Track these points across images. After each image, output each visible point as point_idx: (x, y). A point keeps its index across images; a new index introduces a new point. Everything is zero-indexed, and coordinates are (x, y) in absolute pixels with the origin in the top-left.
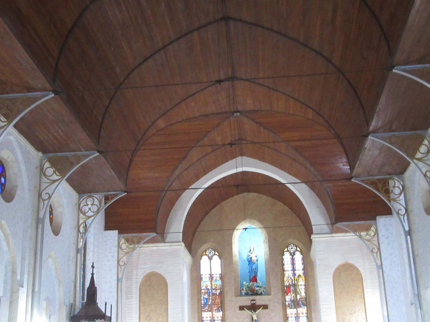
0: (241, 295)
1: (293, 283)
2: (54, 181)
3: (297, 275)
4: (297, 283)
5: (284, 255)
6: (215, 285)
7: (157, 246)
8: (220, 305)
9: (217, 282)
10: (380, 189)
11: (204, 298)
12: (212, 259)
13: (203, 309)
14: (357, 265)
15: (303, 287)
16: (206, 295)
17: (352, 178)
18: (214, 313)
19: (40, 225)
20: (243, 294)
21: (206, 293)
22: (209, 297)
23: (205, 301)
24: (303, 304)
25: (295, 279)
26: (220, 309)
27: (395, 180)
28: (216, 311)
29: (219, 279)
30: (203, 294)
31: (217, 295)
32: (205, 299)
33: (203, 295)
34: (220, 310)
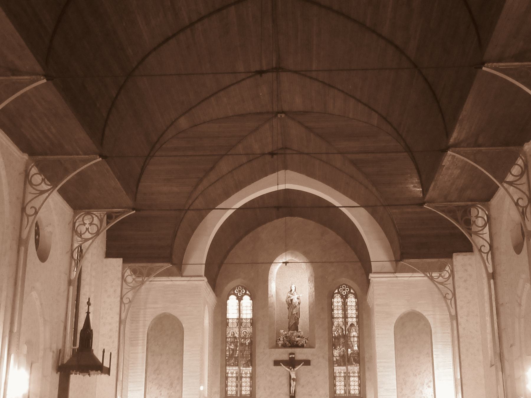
0: (277, 346)
1: (343, 333)
3: (349, 324)
4: (348, 334)
5: (334, 299)
6: (245, 332)
7: (172, 281)
8: (250, 358)
9: (247, 329)
11: (229, 348)
12: (242, 299)
13: (228, 363)
14: (425, 314)
15: (356, 339)
16: (232, 345)
17: (424, 203)
18: (241, 368)
19: (23, 249)
20: (280, 345)
21: (233, 342)
22: (236, 348)
23: (231, 352)
24: (355, 360)
25: (347, 328)
26: (249, 363)
27: (478, 208)
28: (245, 366)
29: (249, 325)
30: (228, 344)
31: (246, 346)
32: (231, 350)
33: (229, 345)
34: (250, 365)
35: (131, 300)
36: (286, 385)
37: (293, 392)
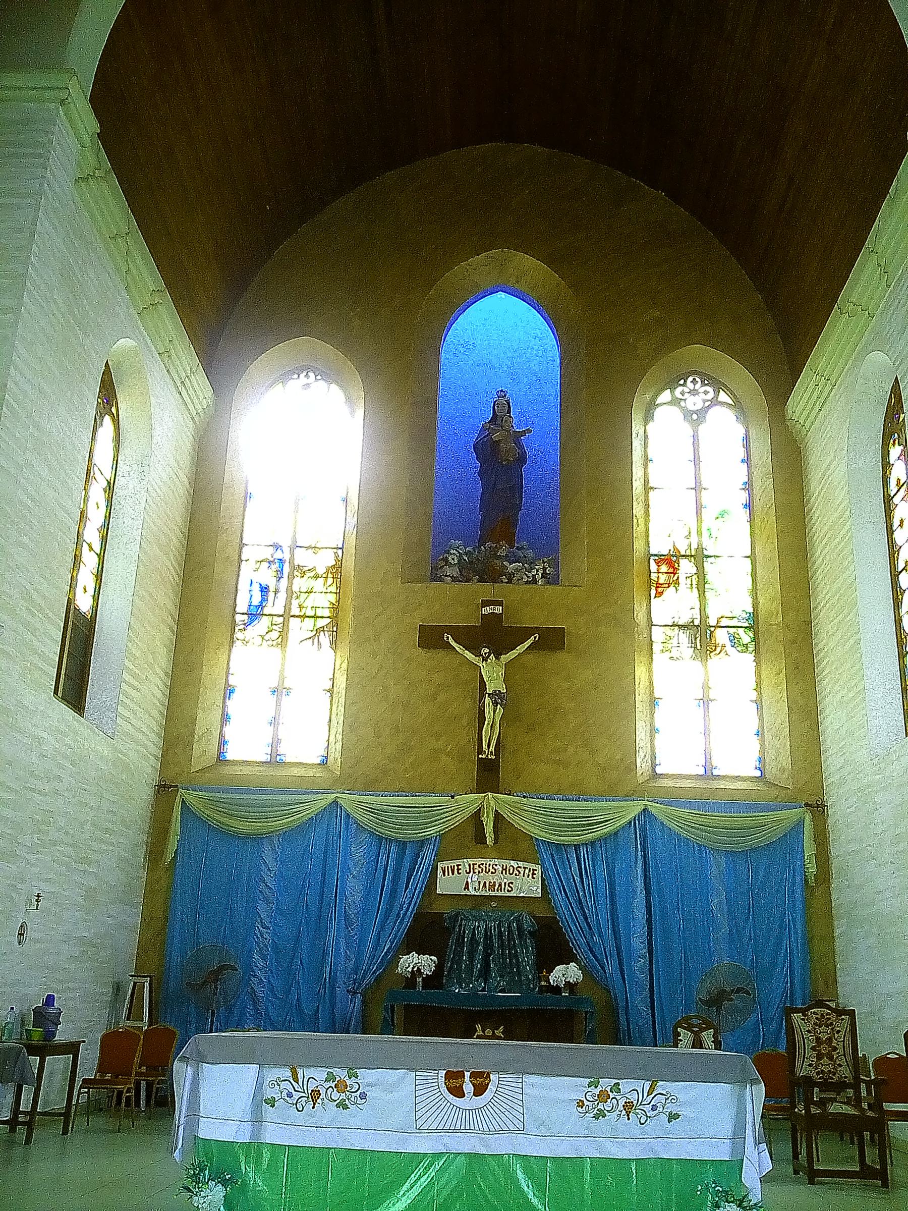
0: (436, 577)
24: (735, 641)
36: (464, 721)
37: (492, 749)
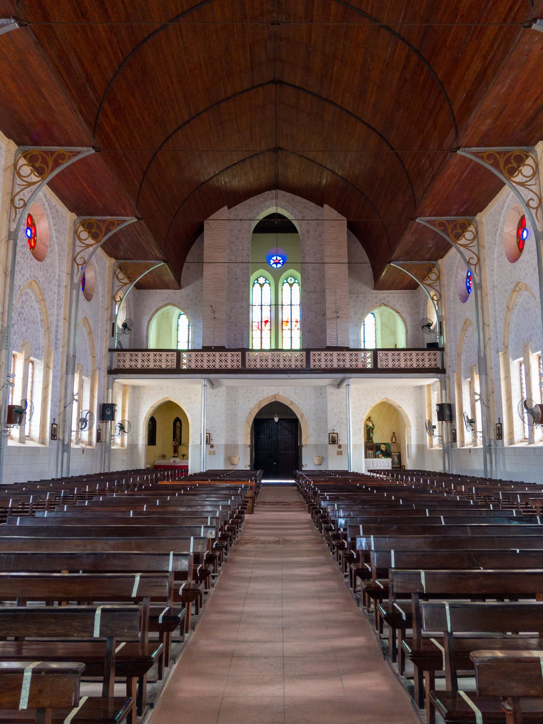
2: (30, 184)
10: (450, 231)
35: (86, 259)
